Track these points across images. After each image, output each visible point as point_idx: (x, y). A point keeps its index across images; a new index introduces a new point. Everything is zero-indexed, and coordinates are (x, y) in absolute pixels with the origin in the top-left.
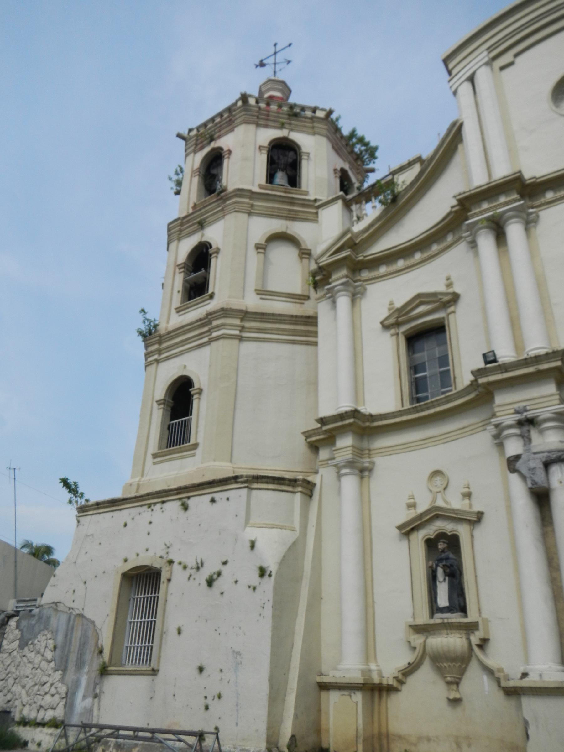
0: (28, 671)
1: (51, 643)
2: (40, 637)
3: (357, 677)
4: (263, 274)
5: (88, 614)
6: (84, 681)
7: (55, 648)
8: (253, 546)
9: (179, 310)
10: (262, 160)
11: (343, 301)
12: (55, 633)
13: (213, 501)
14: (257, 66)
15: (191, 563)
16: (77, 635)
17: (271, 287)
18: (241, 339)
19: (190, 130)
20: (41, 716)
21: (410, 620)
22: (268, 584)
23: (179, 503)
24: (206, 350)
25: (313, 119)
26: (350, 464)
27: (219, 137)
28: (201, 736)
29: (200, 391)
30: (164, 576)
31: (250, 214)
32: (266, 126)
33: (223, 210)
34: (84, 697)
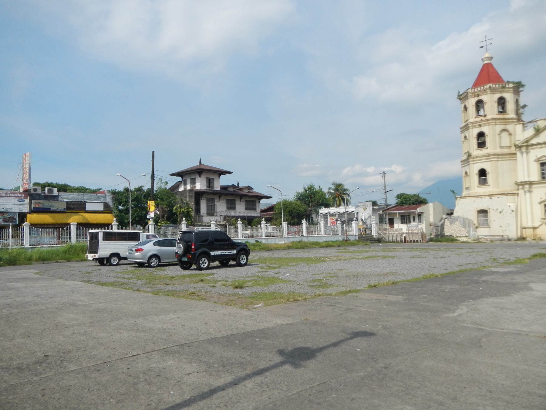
0: (455, 228)
1: (460, 223)
2: (456, 222)
3: (531, 226)
4: (500, 143)
5: (468, 218)
6: (471, 229)
7: (461, 224)
8: (510, 206)
9: (476, 150)
10: (496, 104)
11: (525, 154)
12: (460, 222)
13: (498, 198)
14: (480, 48)
15: (495, 209)
16: (467, 222)
17: (502, 146)
18: (498, 161)
19: (469, 89)
20: (462, 236)
21: (541, 217)
22: (514, 213)
23: (489, 198)
24: (489, 163)
25: (509, 88)
26: (528, 191)
27: (481, 95)
28: (503, 236)
29: (489, 173)
30: (488, 211)
31: (495, 125)
32: (496, 93)
33: (488, 123)
34: (472, 232)
